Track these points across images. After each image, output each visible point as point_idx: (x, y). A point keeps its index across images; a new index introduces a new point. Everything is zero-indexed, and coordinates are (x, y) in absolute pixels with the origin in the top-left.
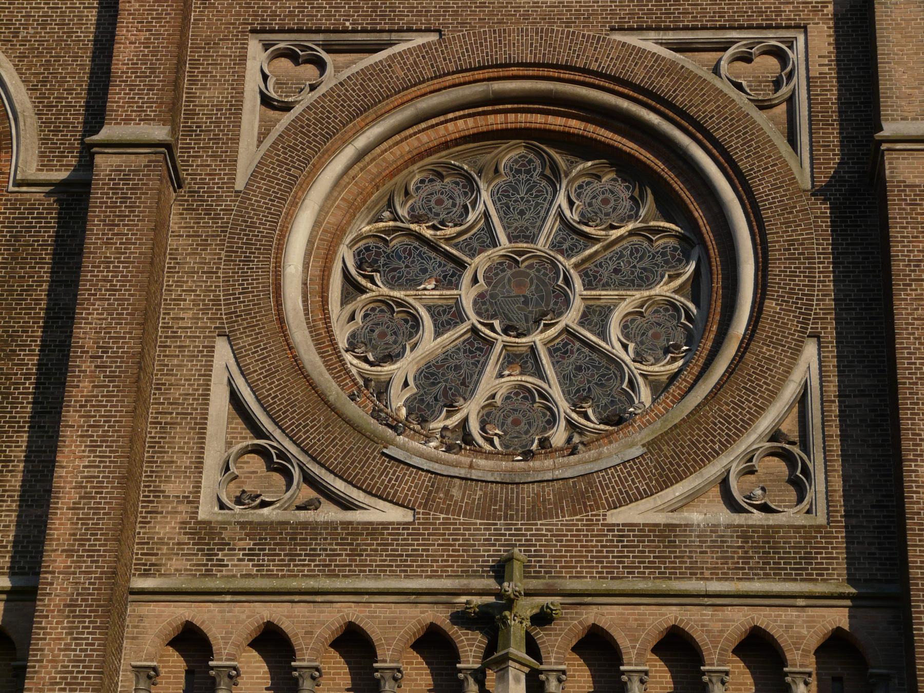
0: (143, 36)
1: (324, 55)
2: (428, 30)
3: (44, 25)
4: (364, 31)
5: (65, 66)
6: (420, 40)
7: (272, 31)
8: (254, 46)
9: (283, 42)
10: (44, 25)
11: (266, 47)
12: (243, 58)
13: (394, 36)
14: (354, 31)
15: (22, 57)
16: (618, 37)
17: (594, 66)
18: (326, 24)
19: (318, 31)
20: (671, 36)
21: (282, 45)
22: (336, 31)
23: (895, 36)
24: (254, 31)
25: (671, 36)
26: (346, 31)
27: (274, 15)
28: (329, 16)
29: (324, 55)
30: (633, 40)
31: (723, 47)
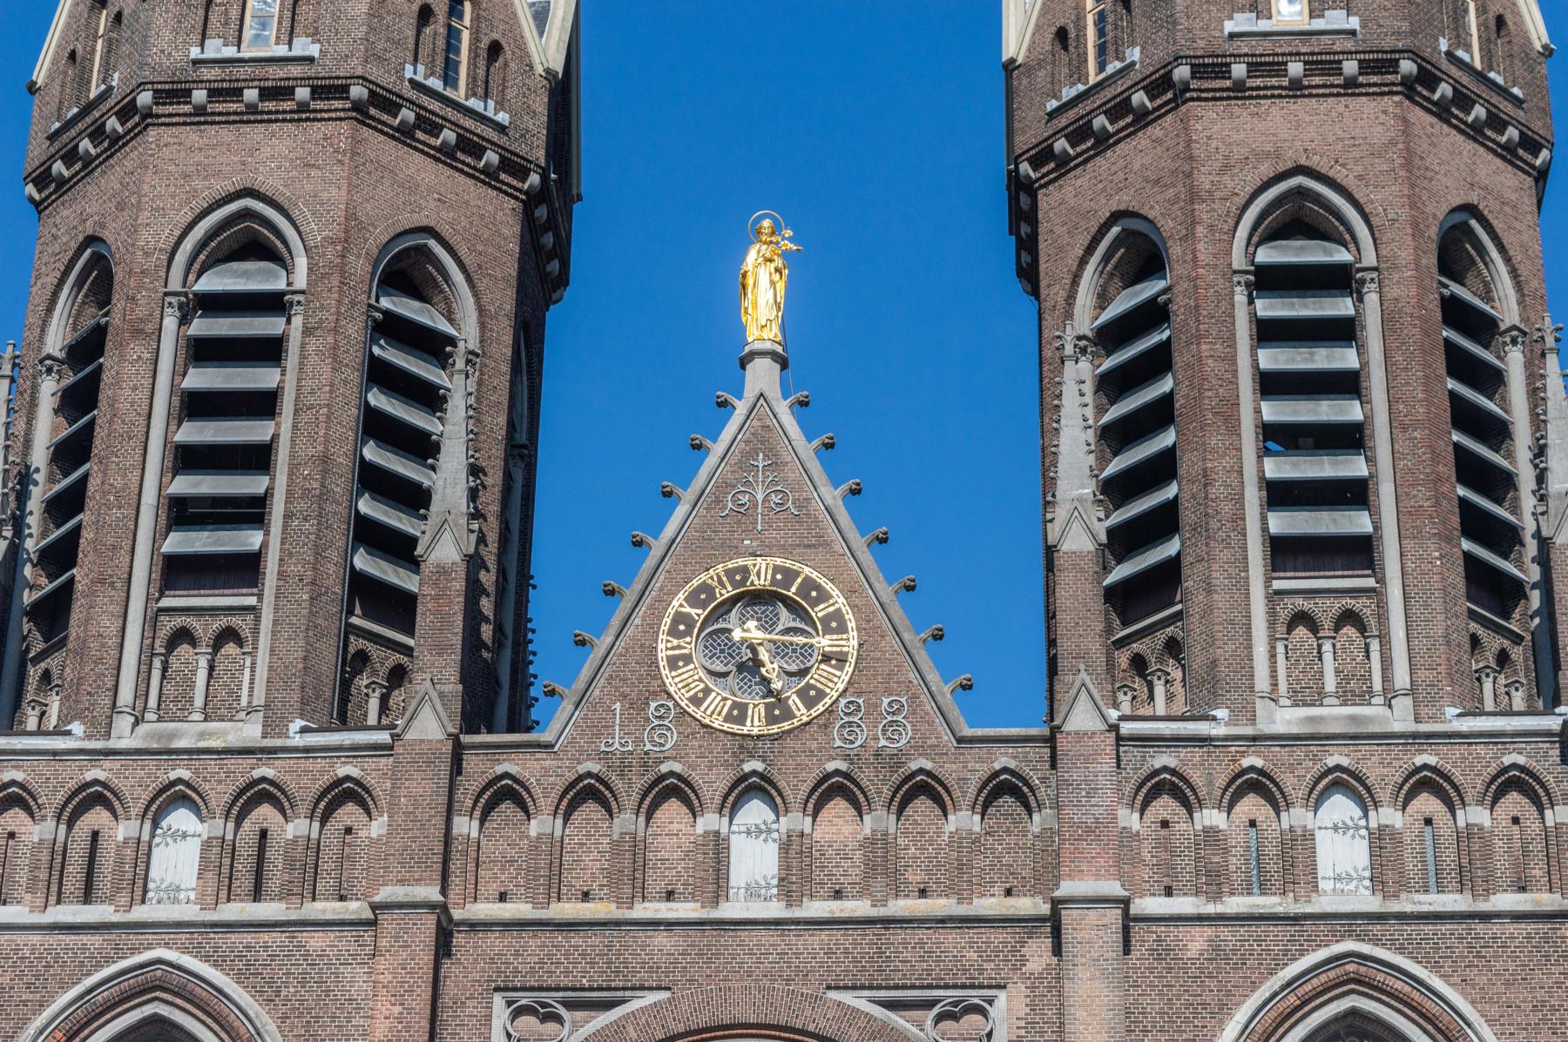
0: (397, 1009)
1: (562, 1011)
2: (659, 988)
3: (303, 983)
4: (600, 989)
5: (324, 1028)
6: (652, 998)
7: (515, 989)
8: (498, 1000)
9: (525, 999)
10: (303, 983)
11: (509, 1003)
12: (489, 1018)
13: (628, 993)
14: (591, 989)
15: (284, 1018)
16: (833, 995)
17: (811, 1028)
18: (566, 981)
19: (557, 989)
20: (883, 994)
21: (524, 1002)
22: (574, 989)
23: (1081, 1014)
24: (497, 989)
25: (883, 994)
26: (583, 989)
27: (516, 971)
28: (567, 973)
29: (562, 1011)
30: (847, 998)
31: (929, 1004)
